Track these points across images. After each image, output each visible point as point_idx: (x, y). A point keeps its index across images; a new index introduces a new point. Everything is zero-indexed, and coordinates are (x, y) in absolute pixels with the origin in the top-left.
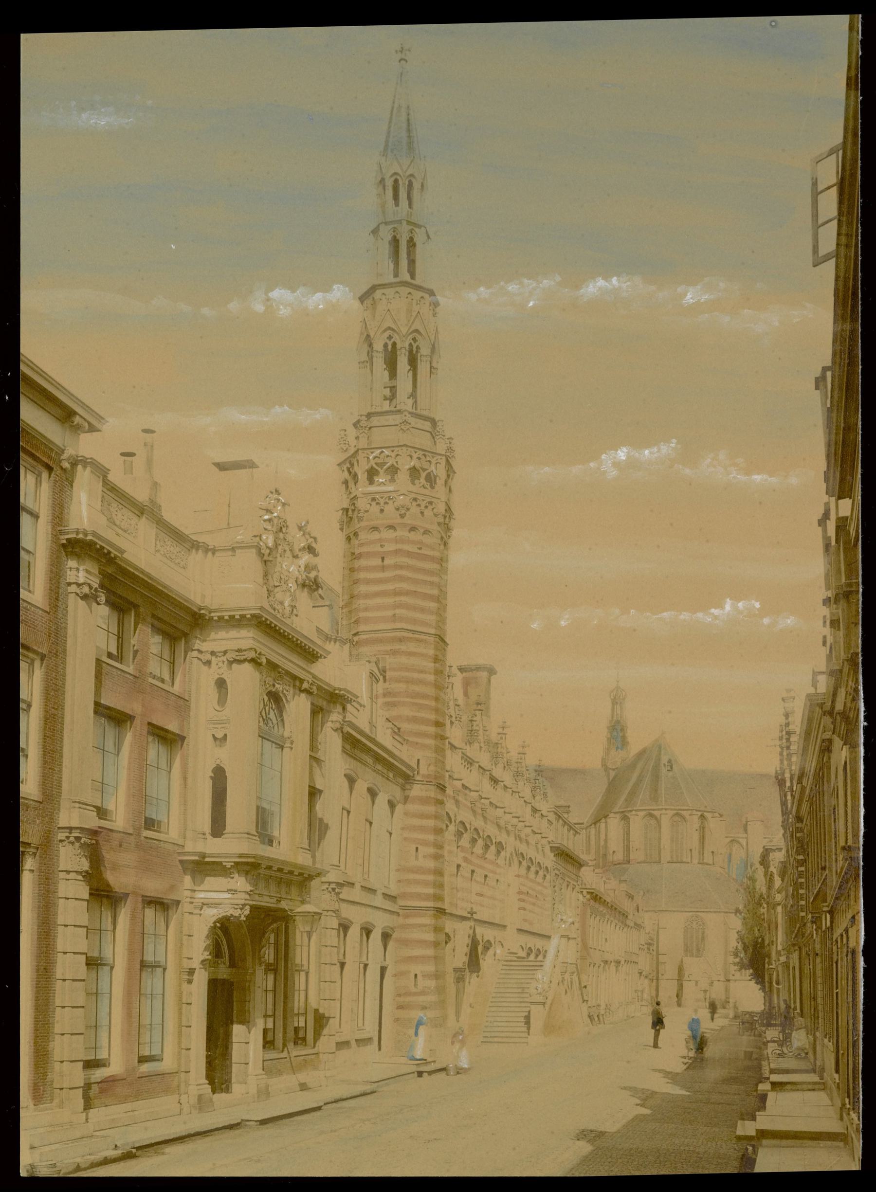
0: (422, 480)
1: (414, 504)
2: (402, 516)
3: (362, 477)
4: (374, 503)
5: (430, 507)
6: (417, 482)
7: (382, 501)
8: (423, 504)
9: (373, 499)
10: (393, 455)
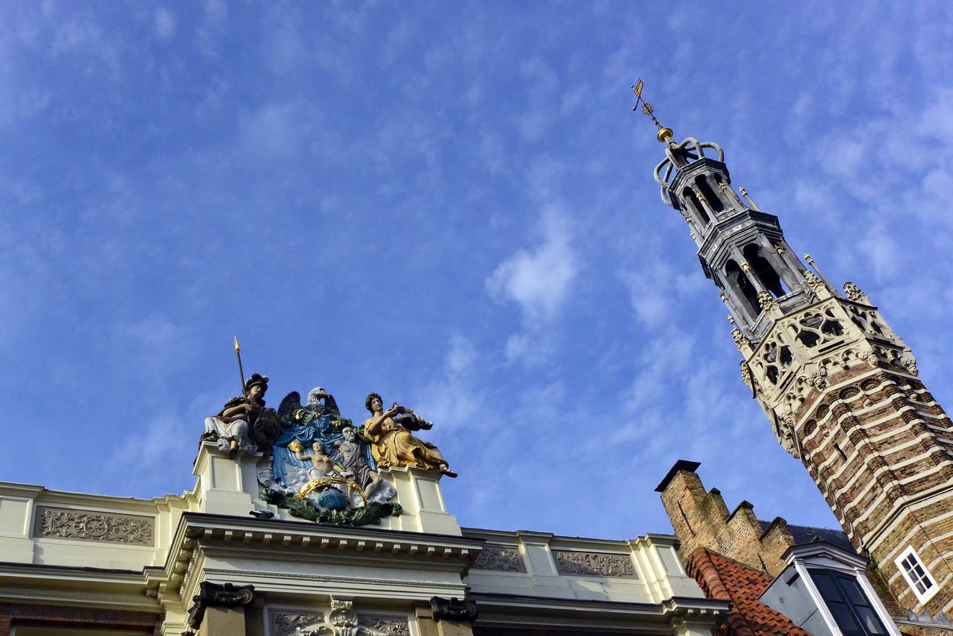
0: (822, 336)
1: (829, 366)
2: (820, 387)
3: (765, 383)
4: (792, 401)
5: (852, 356)
6: (817, 341)
7: (795, 392)
8: (840, 359)
9: (789, 398)
10: (775, 340)
